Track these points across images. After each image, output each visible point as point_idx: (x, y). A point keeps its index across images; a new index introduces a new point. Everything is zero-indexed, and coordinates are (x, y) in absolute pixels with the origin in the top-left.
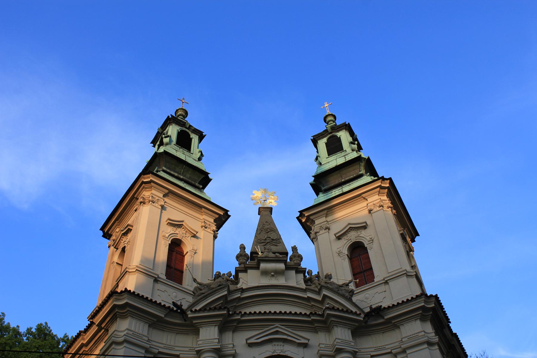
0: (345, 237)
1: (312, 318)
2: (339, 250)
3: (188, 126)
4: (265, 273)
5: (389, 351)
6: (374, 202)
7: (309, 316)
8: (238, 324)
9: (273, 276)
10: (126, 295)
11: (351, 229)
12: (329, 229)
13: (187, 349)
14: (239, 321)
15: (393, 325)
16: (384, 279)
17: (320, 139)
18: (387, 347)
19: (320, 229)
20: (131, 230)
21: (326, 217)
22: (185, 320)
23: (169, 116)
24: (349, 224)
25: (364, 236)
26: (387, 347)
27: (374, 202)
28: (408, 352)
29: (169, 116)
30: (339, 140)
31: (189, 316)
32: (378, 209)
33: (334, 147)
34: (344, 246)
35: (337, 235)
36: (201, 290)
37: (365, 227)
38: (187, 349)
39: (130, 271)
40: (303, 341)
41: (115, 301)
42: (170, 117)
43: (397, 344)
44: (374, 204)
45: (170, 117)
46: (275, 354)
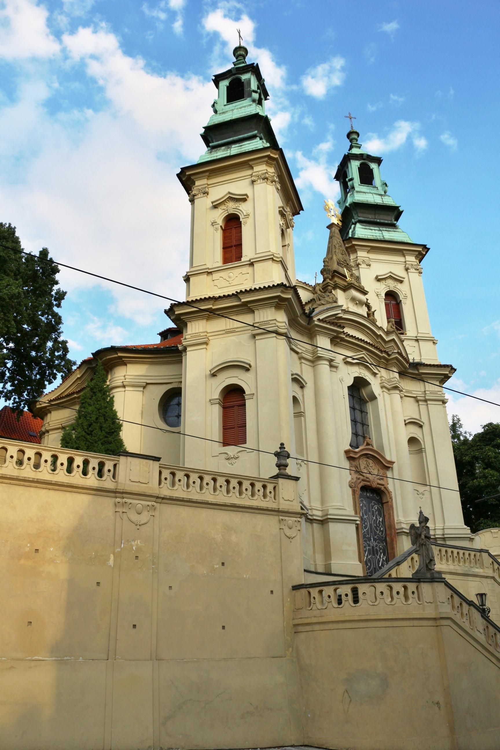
0: (384, 282)
1: (384, 355)
2: (378, 291)
3: (262, 83)
4: (353, 299)
5: (415, 396)
6: (413, 263)
7: (381, 351)
8: (340, 341)
9: (357, 304)
10: (292, 291)
11: (391, 277)
12: (370, 265)
13: (304, 349)
14: (342, 340)
15: (420, 378)
16: (416, 337)
17: (353, 159)
18: (414, 392)
19: (363, 263)
20: (246, 200)
21: (368, 252)
22: (308, 324)
23: (254, 63)
24: (390, 272)
25: (402, 290)
26: (414, 392)
27: (413, 263)
28: (429, 402)
29: (254, 63)
30: (371, 171)
31: (316, 323)
32: (414, 271)
33: (367, 177)
34: (383, 288)
35: (379, 277)
36: (320, 300)
37: (401, 282)
38: (304, 349)
39: (274, 258)
40: (376, 371)
41: (281, 292)
42: (255, 65)
43: (420, 393)
44: (412, 265)
45: (255, 65)
46: (360, 376)
